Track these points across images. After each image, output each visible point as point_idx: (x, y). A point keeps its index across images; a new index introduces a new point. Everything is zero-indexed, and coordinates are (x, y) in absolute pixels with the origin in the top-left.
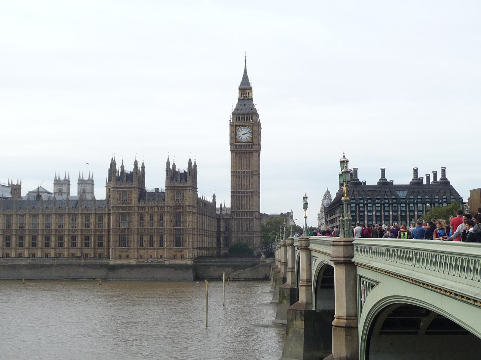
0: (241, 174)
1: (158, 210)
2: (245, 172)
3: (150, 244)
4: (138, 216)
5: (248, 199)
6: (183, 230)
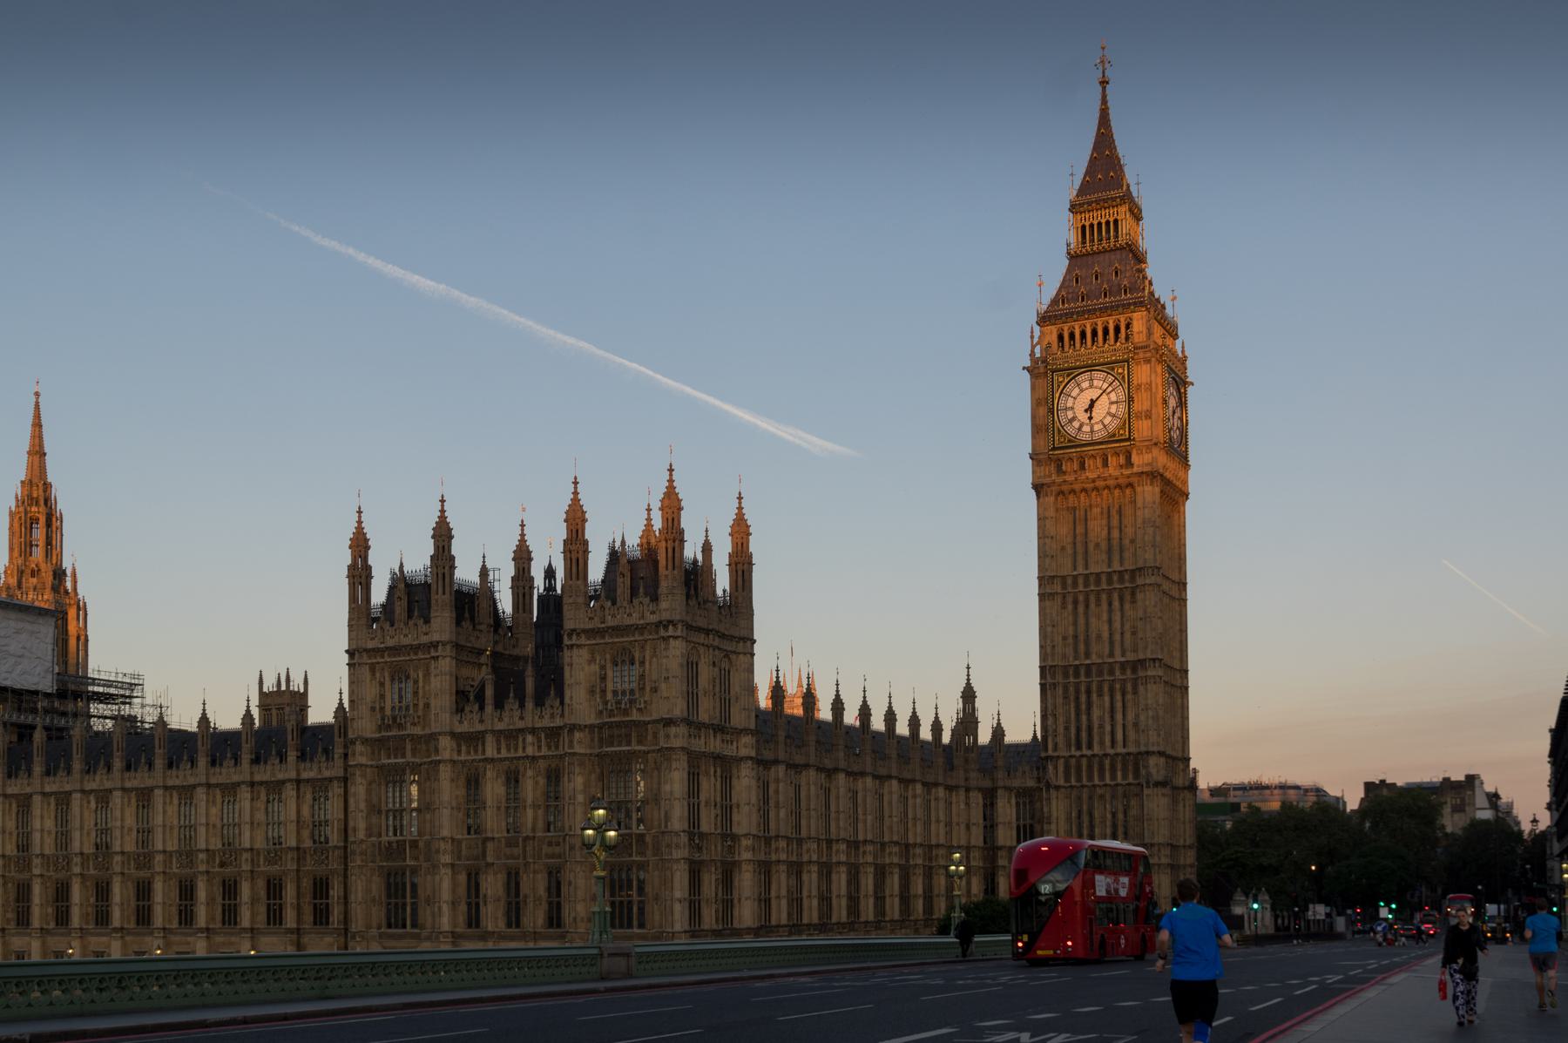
0: (1086, 585)
1: (540, 747)
2: (1104, 578)
3: (508, 913)
4: (452, 780)
5: (1118, 697)
6: (643, 841)
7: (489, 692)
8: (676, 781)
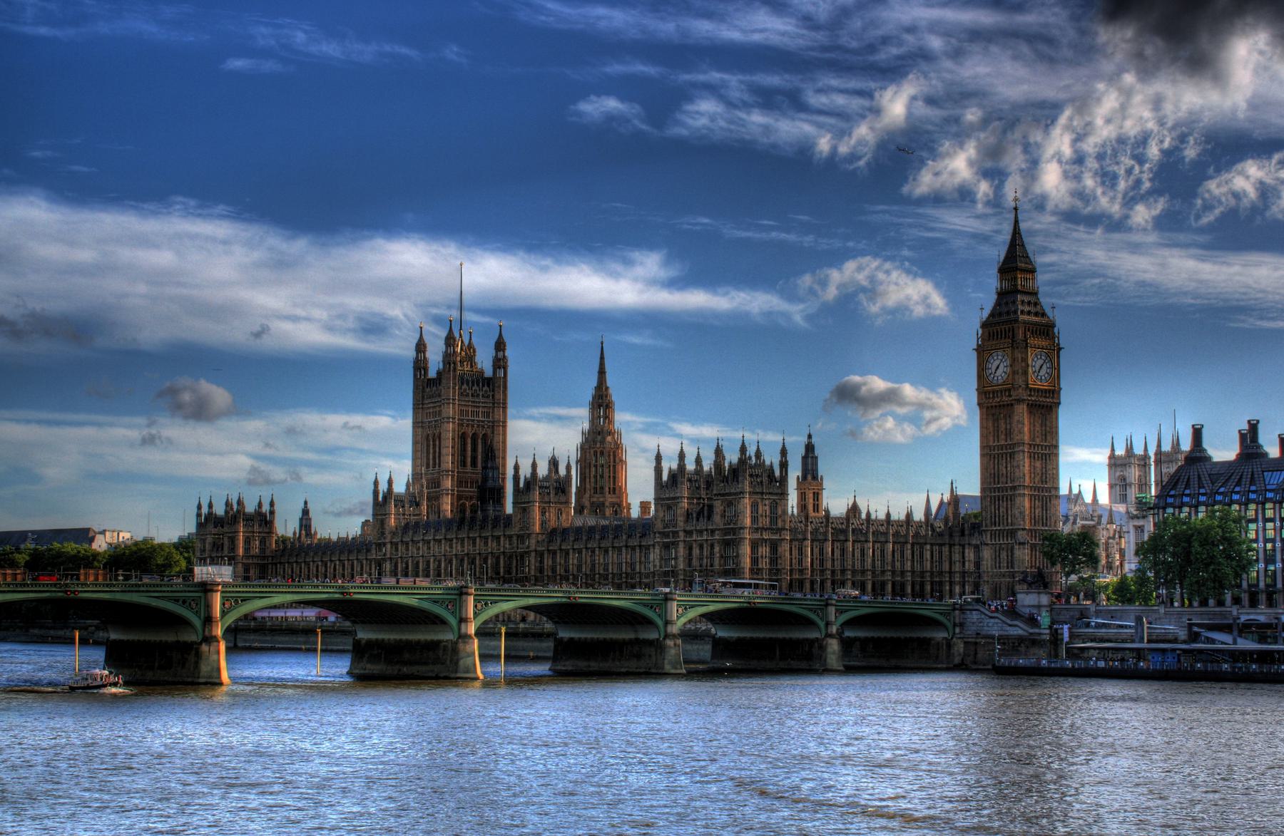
5: (1009, 502)
7: (694, 515)
8: (746, 549)
